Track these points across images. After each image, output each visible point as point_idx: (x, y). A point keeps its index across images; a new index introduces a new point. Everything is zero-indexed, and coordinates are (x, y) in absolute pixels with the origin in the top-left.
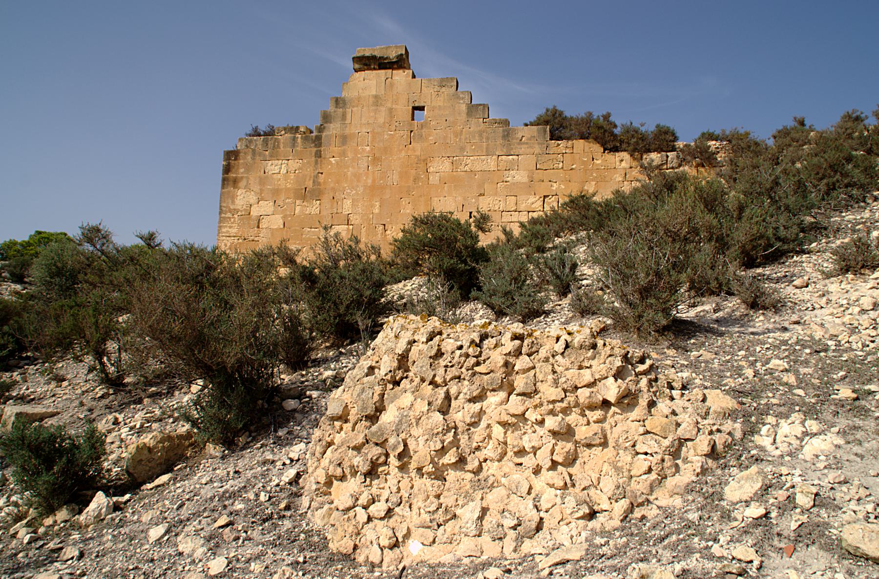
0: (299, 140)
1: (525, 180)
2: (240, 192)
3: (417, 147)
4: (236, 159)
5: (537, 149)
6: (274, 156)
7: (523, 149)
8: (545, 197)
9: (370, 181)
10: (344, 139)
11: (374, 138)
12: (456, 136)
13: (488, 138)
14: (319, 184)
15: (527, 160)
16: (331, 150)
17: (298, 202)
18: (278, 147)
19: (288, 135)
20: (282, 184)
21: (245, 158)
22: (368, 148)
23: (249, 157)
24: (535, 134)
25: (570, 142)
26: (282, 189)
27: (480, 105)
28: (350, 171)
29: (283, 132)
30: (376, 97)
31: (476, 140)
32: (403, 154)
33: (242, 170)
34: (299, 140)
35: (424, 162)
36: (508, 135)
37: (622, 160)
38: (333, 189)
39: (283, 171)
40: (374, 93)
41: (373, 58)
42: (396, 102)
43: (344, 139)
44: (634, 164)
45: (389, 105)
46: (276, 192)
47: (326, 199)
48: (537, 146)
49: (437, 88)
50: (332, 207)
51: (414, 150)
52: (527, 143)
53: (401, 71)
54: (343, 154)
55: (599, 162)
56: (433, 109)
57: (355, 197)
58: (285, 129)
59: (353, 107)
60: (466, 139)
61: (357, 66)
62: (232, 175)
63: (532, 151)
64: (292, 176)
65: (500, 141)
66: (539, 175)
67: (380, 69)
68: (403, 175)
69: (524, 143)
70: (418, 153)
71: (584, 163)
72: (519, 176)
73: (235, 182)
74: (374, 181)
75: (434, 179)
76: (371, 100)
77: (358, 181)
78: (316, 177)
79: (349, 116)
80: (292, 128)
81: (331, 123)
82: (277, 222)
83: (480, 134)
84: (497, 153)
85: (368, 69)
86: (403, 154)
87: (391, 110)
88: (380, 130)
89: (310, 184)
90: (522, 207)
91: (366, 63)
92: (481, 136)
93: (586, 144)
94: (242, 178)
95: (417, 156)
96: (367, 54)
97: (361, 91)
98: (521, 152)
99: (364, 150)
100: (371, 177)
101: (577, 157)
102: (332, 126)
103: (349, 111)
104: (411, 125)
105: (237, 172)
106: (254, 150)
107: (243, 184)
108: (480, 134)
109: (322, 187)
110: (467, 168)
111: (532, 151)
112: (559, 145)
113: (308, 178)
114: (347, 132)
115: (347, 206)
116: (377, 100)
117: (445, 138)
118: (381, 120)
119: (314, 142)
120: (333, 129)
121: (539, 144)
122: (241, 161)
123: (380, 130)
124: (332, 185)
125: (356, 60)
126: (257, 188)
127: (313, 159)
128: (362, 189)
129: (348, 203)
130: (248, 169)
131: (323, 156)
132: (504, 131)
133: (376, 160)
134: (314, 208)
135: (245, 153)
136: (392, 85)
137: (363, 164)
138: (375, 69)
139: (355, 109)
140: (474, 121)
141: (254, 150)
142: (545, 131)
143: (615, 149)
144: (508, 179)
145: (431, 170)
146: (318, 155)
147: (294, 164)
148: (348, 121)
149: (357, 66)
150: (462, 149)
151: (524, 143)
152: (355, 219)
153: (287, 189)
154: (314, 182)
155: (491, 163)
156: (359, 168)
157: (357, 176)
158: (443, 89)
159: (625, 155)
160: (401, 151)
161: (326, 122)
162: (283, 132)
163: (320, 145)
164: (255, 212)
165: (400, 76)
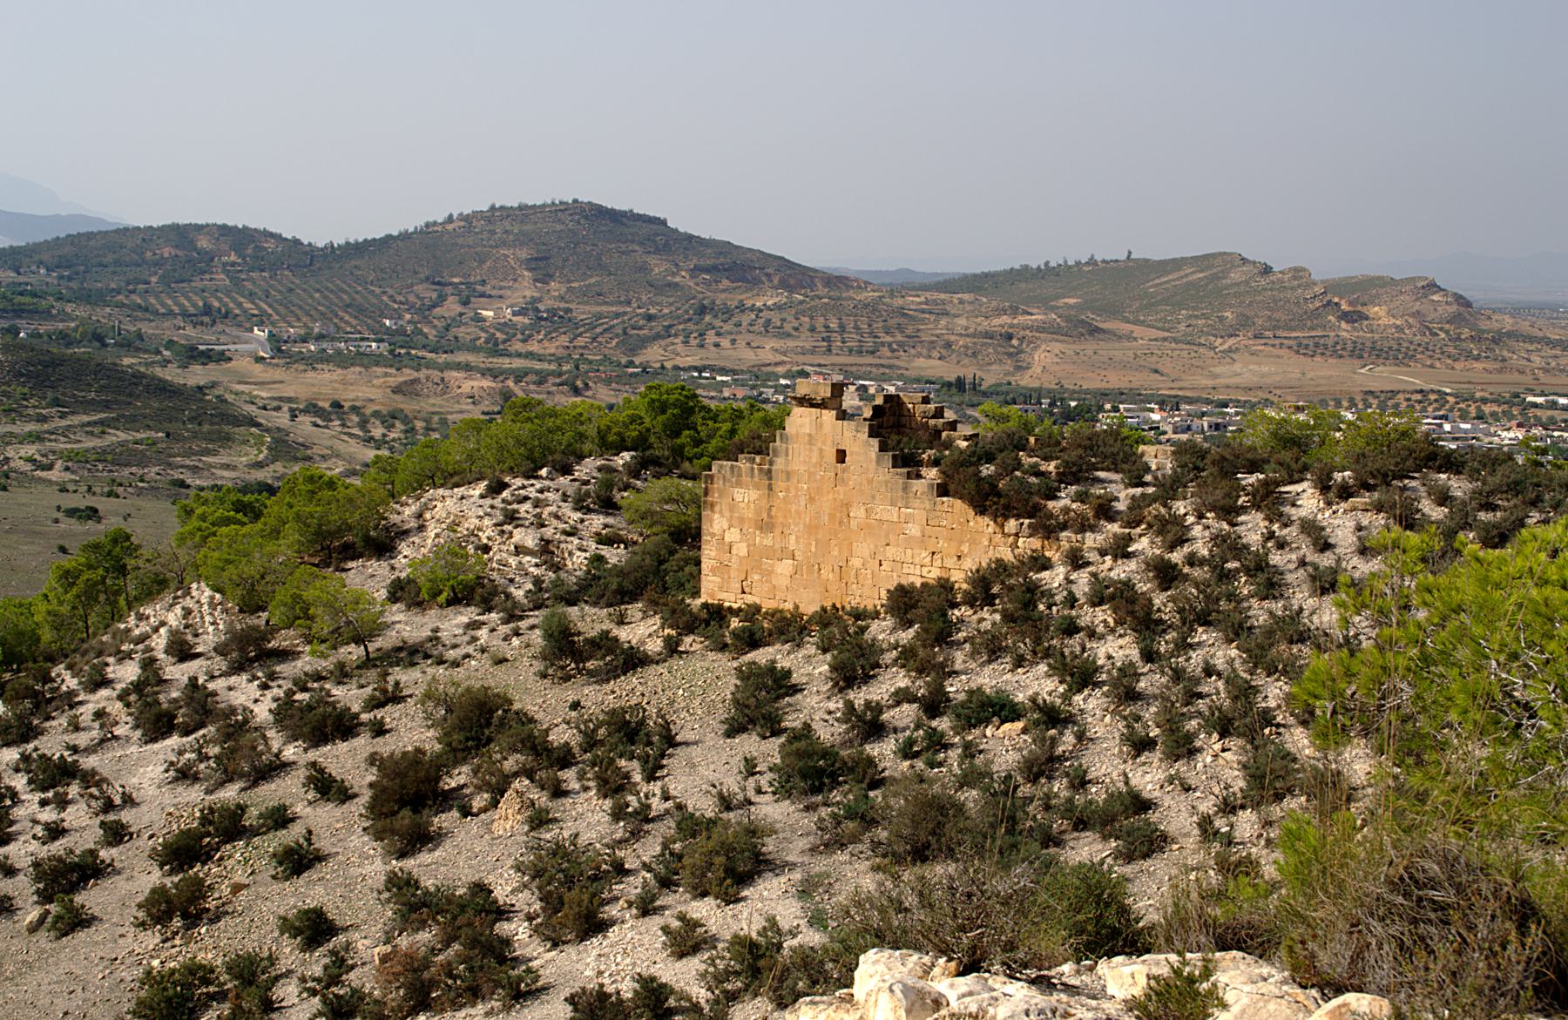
1: (919, 534)
2: (716, 516)
6: (739, 484)
7: (917, 503)
15: (920, 515)
16: (779, 484)
28: (793, 508)
35: (847, 505)
42: (824, 443)
46: (742, 520)
47: (778, 531)
54: (788, 490)
65: (900, 493)
68: (832, 517)
72: (914, 530)
75: (854, 524)
82: (741, 549)
83: (887, 482)
89: (765, 516)
90: (917, 560)
107: (717, 508)
115: (792, 543)
129: (793, 538)
133: (812, 499)
137: (803, 503)
146: (770, 488)
150: (873, 497)
155: (892, 514)
157: (798, 513)
164: (727, 539)
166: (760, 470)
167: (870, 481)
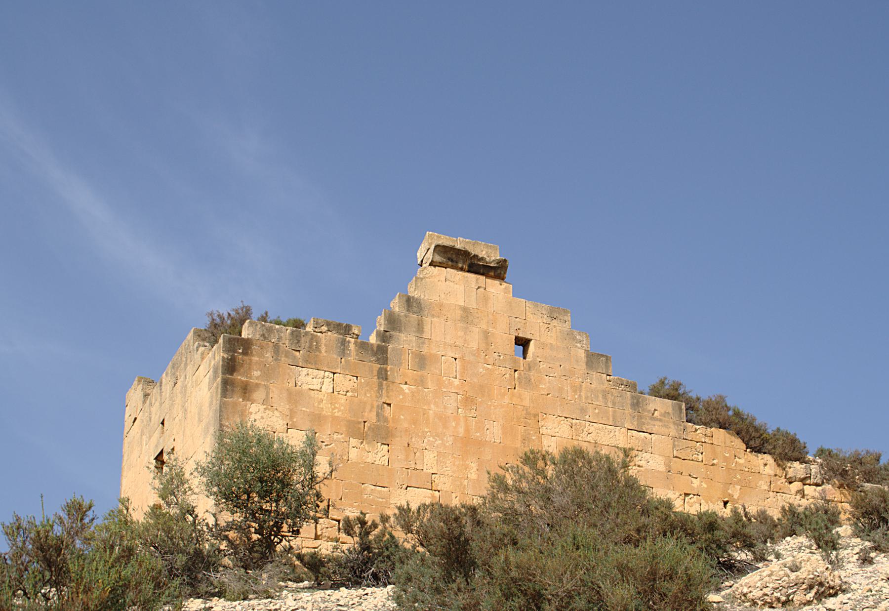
0: (352, 346)
1: (662, 468)
3: (527, 397)
4: (245, 353)
5: (673, 432)
6: (312, 361)
7: (656, 427)
8: (687, 495)
9: (461, 430)
10: (422, 361)
11: (464, 368)
12: (575, 391)
13: (614, 404)
14: (386, 420)
16: (403, 370)
17: (353, 442)
18: (318, 348)
19: (333, 336)
20: (326, 408)
21: (261, 355)
22: (456, 382)
23: (268, 355)
24: (670, 410)
25: (709, 430)
26: (325, 417)
27: (602, 356)
29: (324, 328)
30: (465, 310)
31: (600, 401)
32: (507, 400)
33: (257, 373)
34: (352, 346)
36: (638, 404)
37: (766, 465)
38: (407, 430)
39: (327, 387)
40: (463, 304)
41: (465, 254)
43: (422, 361)
44: (779, 471)
45: (484, 326)
47: (398, 443)
48: (672, 426)
49: (546, 319)
50: (407, 459)
51: (520, 396)
52: (660, 420)
53: (497, 282)
54: (421, 382)
55: (741, 461)
56: (542, 346)
57: (441, 450)
58: (328, 324)
59: (433, 316)
60: (587, 398)
61: (438, 258)
62: (239, 377)
63: (666, 431)
64: (343, 400)
65: (629, 410)
66: (677, 465)
67: (468, 271)
69: (656, 419)
70: (527, 403)
71: (726, 459)
73: (246, 390)
74: (467, 430)
76: (459, 313)
77: (445, 426)
78: (382, 408)
79: (427, 328)
80: (340, 325)
81: (400, 331)
83: (605, 394)
84: (627, 426)
85: (452, 267)
86: (507, 400)
87: (486, 334)
88: (472, 358)
89: (372, 417)
91: (452, 258)
92: (605, 397)
93: (728, 436)
94: (257, 385)
95: (525, 408)
96: (458, 246)
97: (443, 296)
98: (654, 430)
99: (451, 384)
100: (462, 423)
101: (718, 449)
102: (402, 336)
103: (427, 320)
104: (515, 361)
105: (248, 373)
106: (276, 347)
107: (259, 395)
108: (605, 394)
109: (391, 425)
110: (589, 438)
111: (666, 431)
112: (696, 430)
113: (368, 407)
114: (425, 350)
115: (429, 461)
116: (467, 315)
117: (561, 390)
118: (474, 345)
119: (375, 354)
120: (404, 341)
121: (675, 424)
122: (255, 359)
123: (472, 358)
124: (406, 425)
125: (441, 249)
126: (285, 407)
127: (375, 379)
128: (450, 439)
130: (268, 373)
131: (390, 379)
132: (633, 397)
133: (468, 401)
134: (378, 454)
135: (262, 347)
136: (486, 299)
138: (462, 269)
139: (435, 319)
140: (595, 375)
141: (276, 347)
142: (680, 409)
143: (758, 450)
144: (641, 463)
145: (544, 430)
146: (383, 375)
147: (345, 382)
148: (426, 335)
149: (438, 258)
150: (583, 411)
151: (656, 419)
152: (442, 483)
153: (334, 418)
154: (378, 415)
156: (445, 408)
157: (443, 419)
158: (555, 323)
159: (768, 458)
160: (504, 395)
161: (394, 329)
162: (324, 328)
163: (385, 361)
165: (494, 287)
166: (363, 346)
167: (576, 389)
